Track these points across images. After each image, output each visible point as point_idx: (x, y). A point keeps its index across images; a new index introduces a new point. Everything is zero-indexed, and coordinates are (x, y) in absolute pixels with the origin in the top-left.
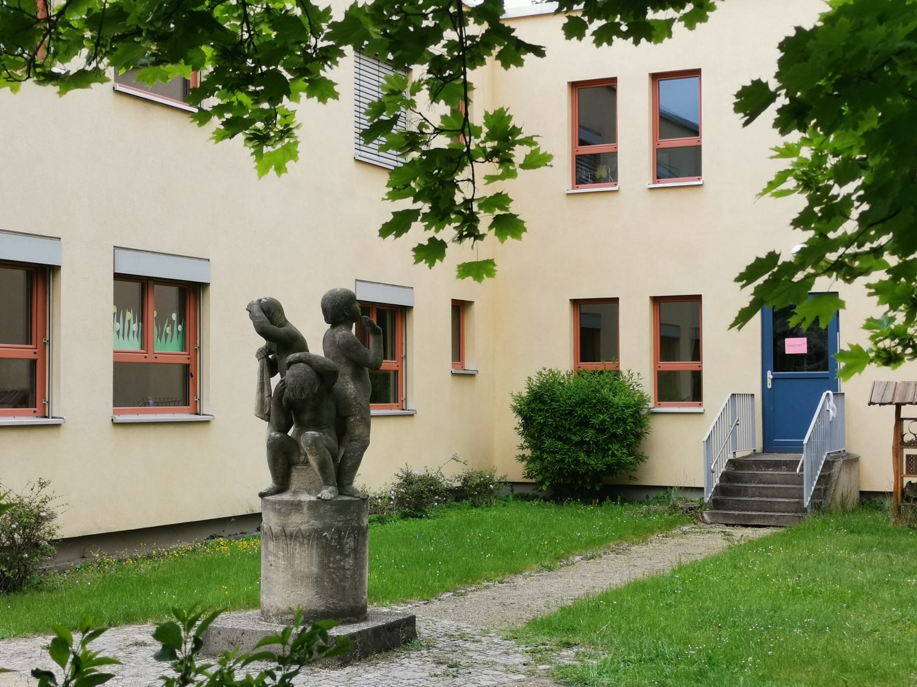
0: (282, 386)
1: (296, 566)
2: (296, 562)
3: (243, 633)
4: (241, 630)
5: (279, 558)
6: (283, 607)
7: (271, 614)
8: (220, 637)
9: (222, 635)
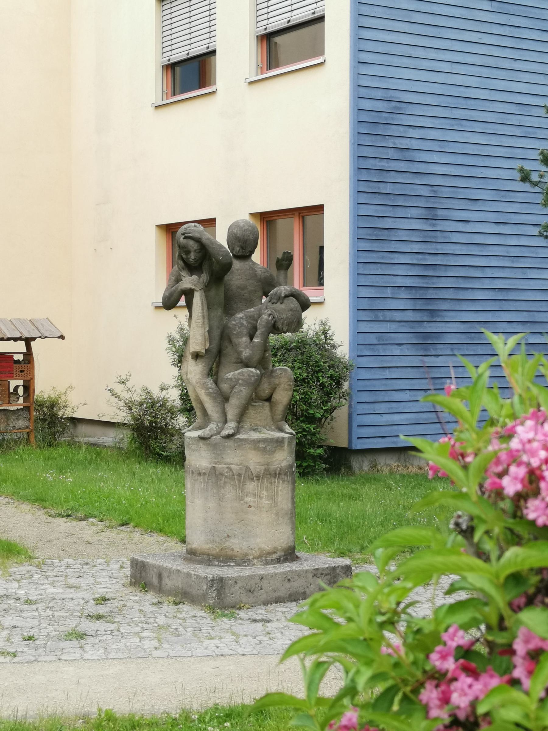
0: (272, 319)
1: (279, 504)
2: (279, 500)
3: (262, 578)
4: (259, 575)
5: (261, 498)
6: (268, 547)
7: (251, 557)
8: (237, 587)
9: (240, 584)
